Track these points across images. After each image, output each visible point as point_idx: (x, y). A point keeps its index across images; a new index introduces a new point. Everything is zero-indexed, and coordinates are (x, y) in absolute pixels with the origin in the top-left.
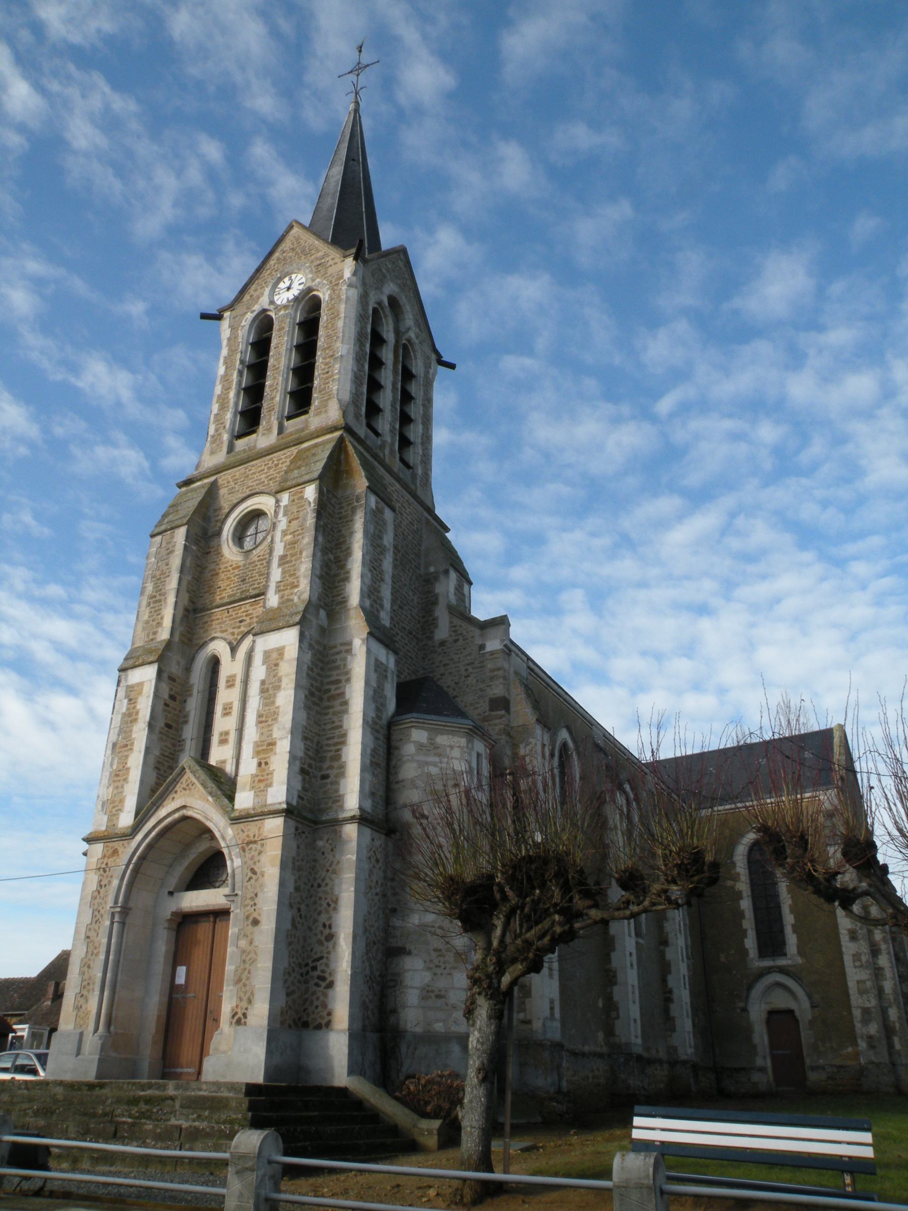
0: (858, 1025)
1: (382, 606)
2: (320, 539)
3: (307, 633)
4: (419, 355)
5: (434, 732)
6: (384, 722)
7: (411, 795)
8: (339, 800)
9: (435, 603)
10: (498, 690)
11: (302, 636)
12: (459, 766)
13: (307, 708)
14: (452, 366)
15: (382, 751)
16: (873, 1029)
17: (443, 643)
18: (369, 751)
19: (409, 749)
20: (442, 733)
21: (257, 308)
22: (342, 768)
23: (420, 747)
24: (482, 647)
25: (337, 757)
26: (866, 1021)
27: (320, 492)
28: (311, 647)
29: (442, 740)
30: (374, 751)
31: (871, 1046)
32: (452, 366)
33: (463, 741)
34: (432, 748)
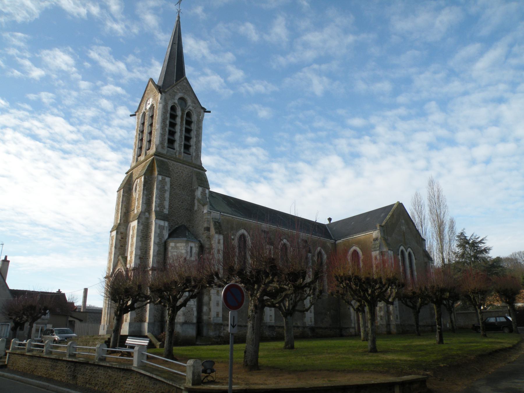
0: (378, 312)
1: (164, 208)
2: (145, 192)
3: (141, 221)
4: (194, 113)
5: (176, 243)
6: (163, 241)
7: (170, 261)
8: (148, 265)
9: (195, 198)
10: (206, 225)
11: (138, 222)
12: (184, 251)
13: (141, 241)
14: (210, 112)
15: (162, 250)
16: (382, 313)
17: (196, 211)
18: (156, 251)
19: (170, 248)
20: (178, 243)
21: (143, 111)
22: (150, 256)
23: (172, 247)
24: (203, 212)
25: (149, 253)
26: (380, 311)
27: (145, 178)
28: (142, 224)
29: (178, 245)
30: (158, 251)
31: (381, 319)
32: (210, 112)
33: (184, 244)
34: (176, 247)
